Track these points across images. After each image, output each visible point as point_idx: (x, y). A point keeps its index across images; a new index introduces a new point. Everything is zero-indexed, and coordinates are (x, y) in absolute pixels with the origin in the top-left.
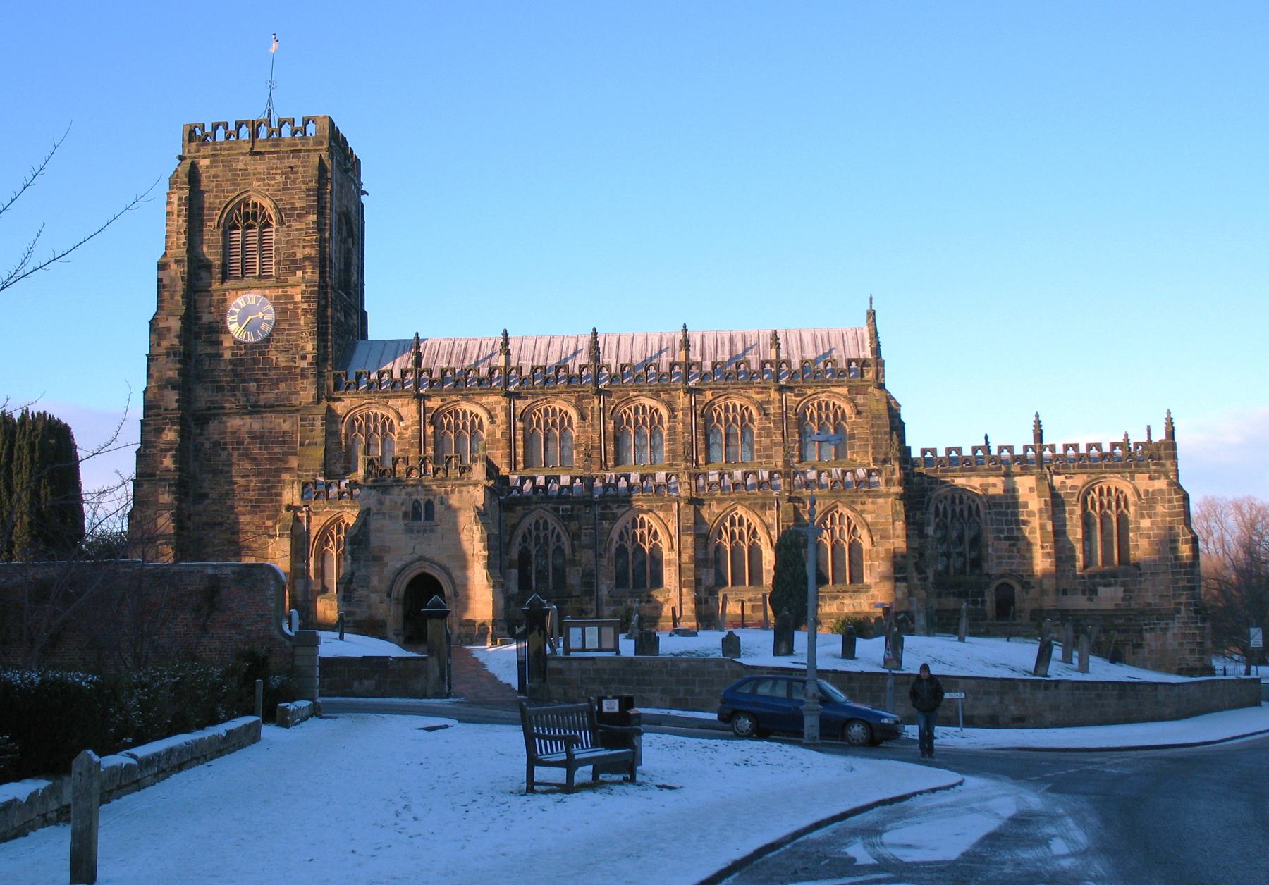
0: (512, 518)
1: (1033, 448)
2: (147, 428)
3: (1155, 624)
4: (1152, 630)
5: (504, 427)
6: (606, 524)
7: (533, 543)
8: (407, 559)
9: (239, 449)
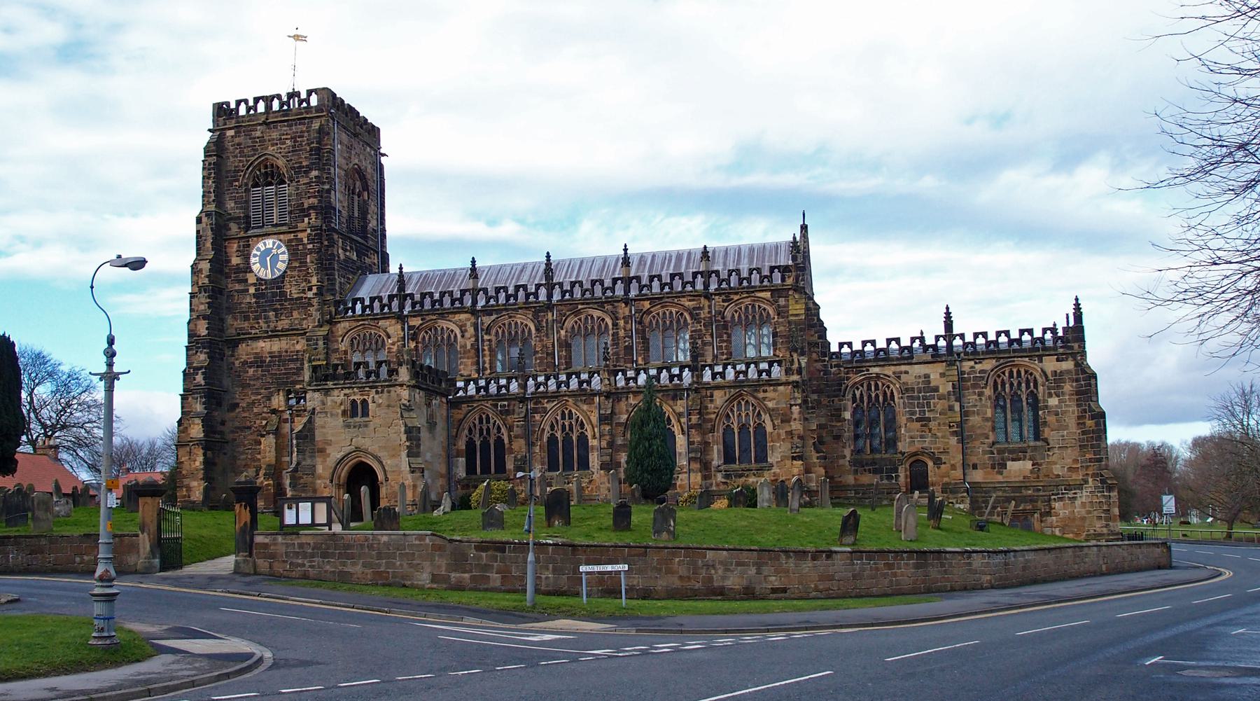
0: (458, 414)
1: (944, 337)
2: (191, 352)
3: (1063, 494)
4: (1061, 499)
5: (473, 339)
6: (537, 417)
7: (478, 435)
8: (348, 449)
9: (262, 367)
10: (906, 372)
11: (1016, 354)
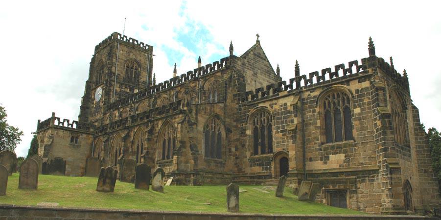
10: (276, 104)
11: (333, 83)
